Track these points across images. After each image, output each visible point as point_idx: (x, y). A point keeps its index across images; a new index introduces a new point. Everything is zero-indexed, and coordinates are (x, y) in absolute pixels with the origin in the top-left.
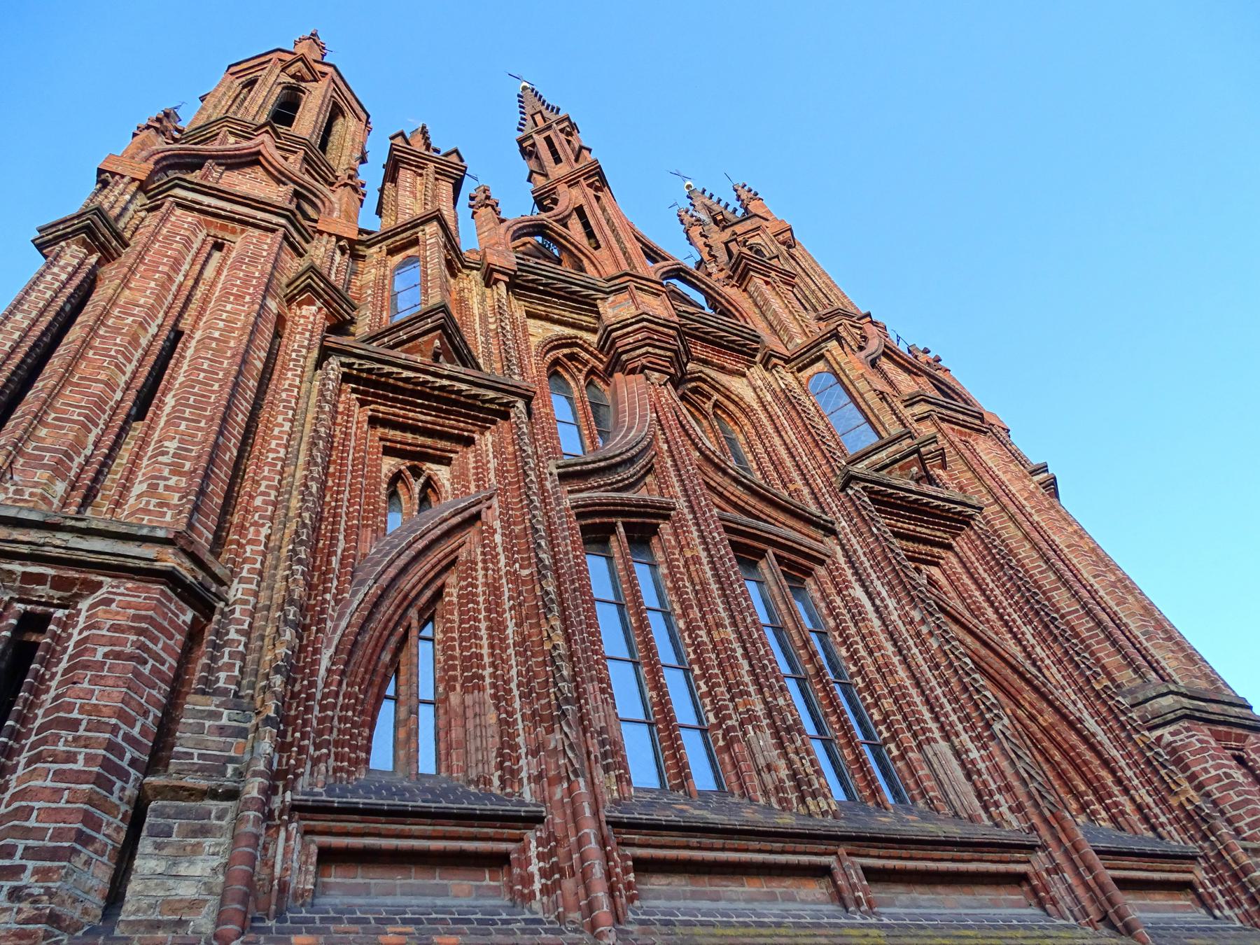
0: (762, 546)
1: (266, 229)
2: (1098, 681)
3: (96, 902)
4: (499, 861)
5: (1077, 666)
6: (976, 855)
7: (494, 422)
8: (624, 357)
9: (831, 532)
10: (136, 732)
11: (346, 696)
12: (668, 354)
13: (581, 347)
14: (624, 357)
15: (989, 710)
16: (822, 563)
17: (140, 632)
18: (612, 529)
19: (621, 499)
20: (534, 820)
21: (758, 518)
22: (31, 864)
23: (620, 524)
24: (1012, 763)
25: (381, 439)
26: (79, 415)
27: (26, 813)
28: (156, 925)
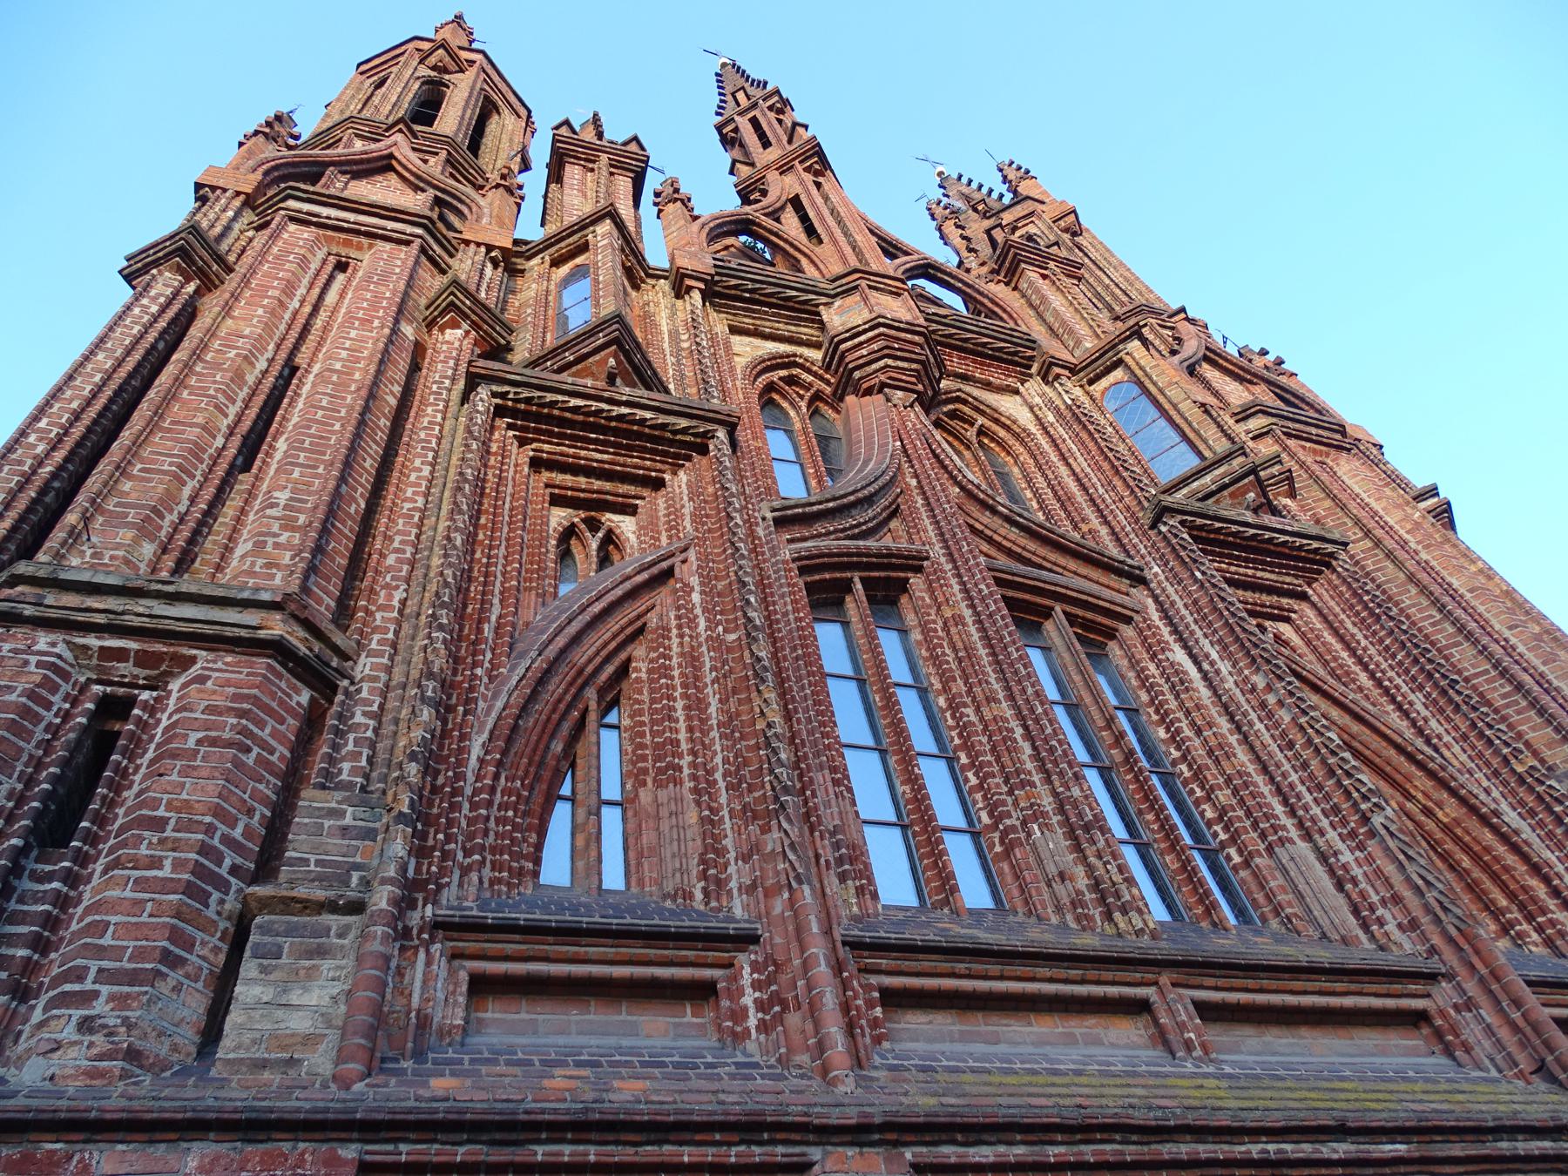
0: (1048, 602)
1: (399, 242)
2: (1521, 762)
3: (188, 1037)
4: (703, 992)
5: (1490, 742)
6: (1353, 987)
7: (689, 458)
8: (857, 374)
9: (1140, 580)
10: (237, 833)
11: (507, 792)
12: (914, 366)
13: (802, 367)
14: (857, 374)
15: (1365, 798)
16: (1128, 620)
17: (242, 714)
18: (847, 586)
19: (858, 547)
20: (747, 939)
21: (1041, 567)
22: (105, 990)
23: (857, 580)
24: (1401, 866)
25: (547, 486)
26: (171, 464)
27: (100, 928)
28: (263, 1065)
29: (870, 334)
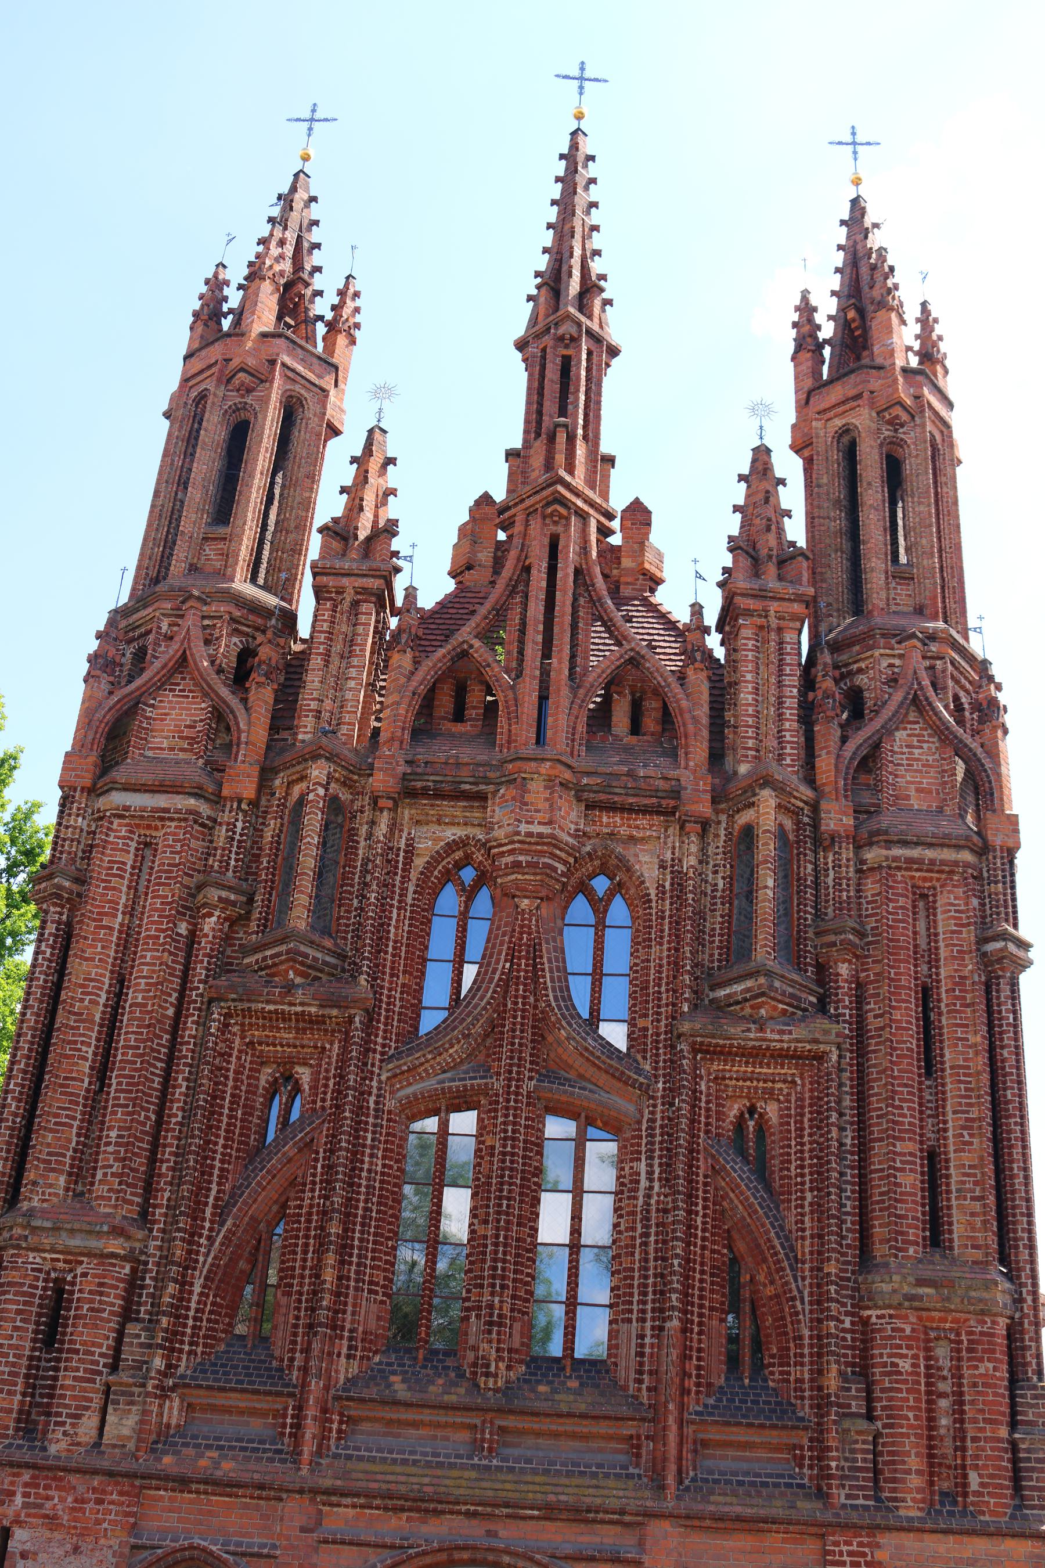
1: (180, 820)
17: (101, 1294)
22: (69, 1421)
28: (114, 1446)
29: (510, 847)
